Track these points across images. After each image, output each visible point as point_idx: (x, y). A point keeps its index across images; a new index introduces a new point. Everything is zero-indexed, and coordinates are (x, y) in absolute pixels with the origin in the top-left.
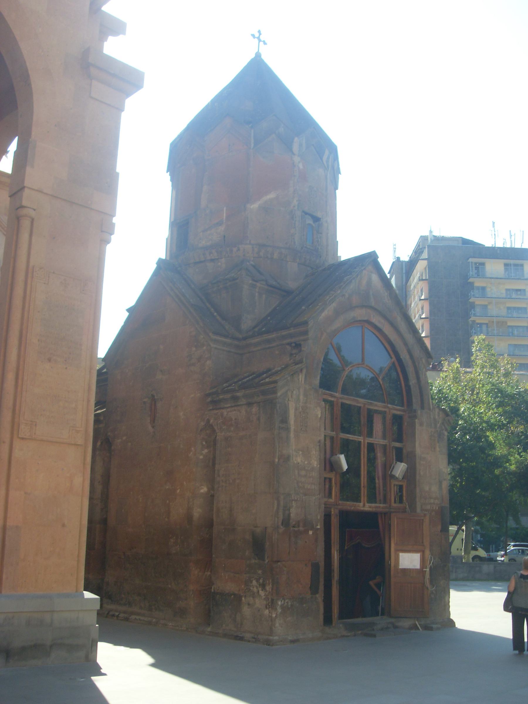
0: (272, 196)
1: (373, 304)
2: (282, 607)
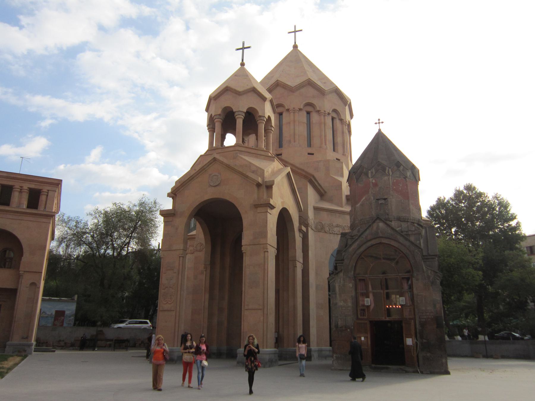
0: (364, 198)
1: (381, 235)
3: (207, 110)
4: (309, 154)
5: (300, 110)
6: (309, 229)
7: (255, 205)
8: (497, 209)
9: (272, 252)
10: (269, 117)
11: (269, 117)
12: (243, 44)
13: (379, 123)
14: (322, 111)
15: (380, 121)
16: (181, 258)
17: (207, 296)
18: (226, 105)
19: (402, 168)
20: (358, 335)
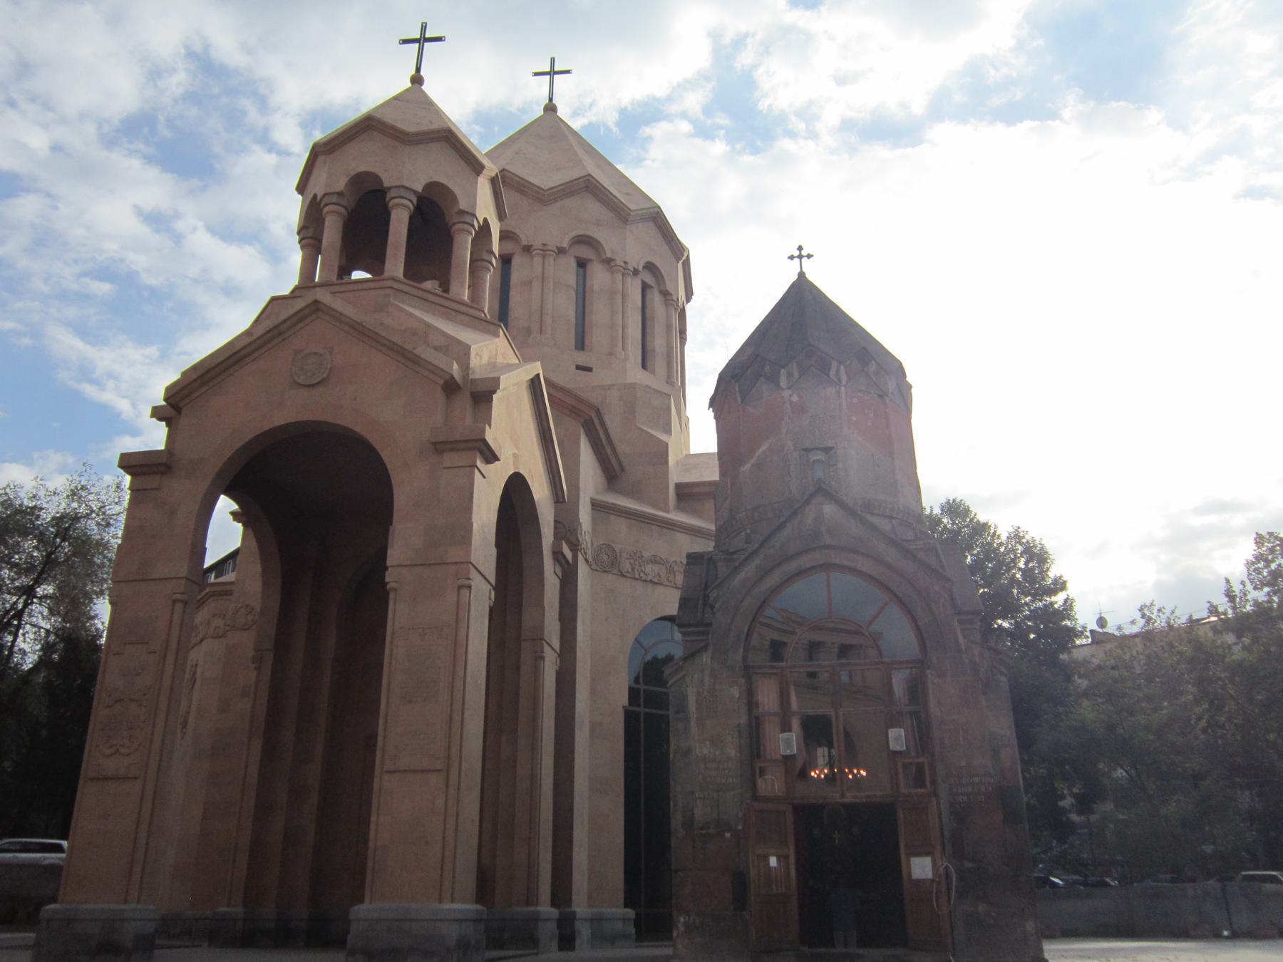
2: (686, 925)
3: (301, 188)
4: (578, 367)
5: (561, 251)
6: (580, 558)
7: (434, 444)
8: (1021, 565)
9: (482, 595)
10: (485, 220)
11: (485, 220)
12: (424, 27)
13: (800, 257)
15: (804, 253)
16: (179, 607)
17: (257, 745)
18: (363, 168)
19: (873, 367)
20: (759, 851)
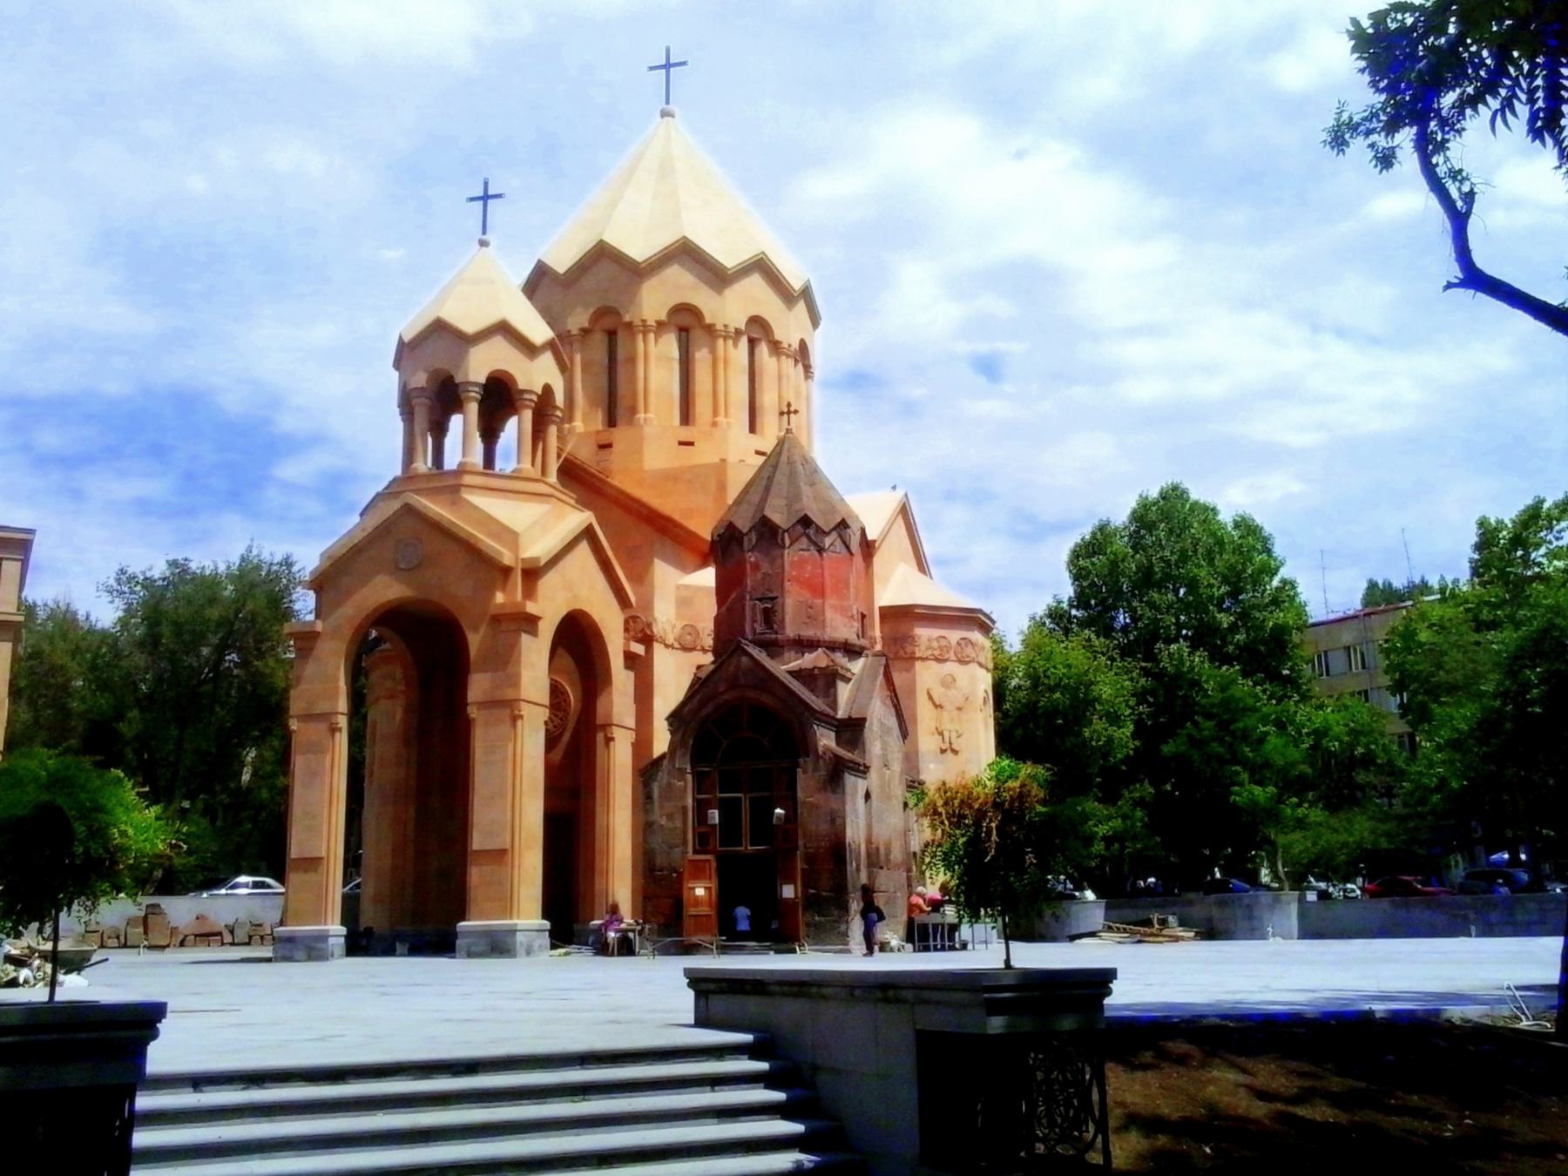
4: (681, 443)
11: (548, 390)
13: (789, 413)
14: (719, 327)
